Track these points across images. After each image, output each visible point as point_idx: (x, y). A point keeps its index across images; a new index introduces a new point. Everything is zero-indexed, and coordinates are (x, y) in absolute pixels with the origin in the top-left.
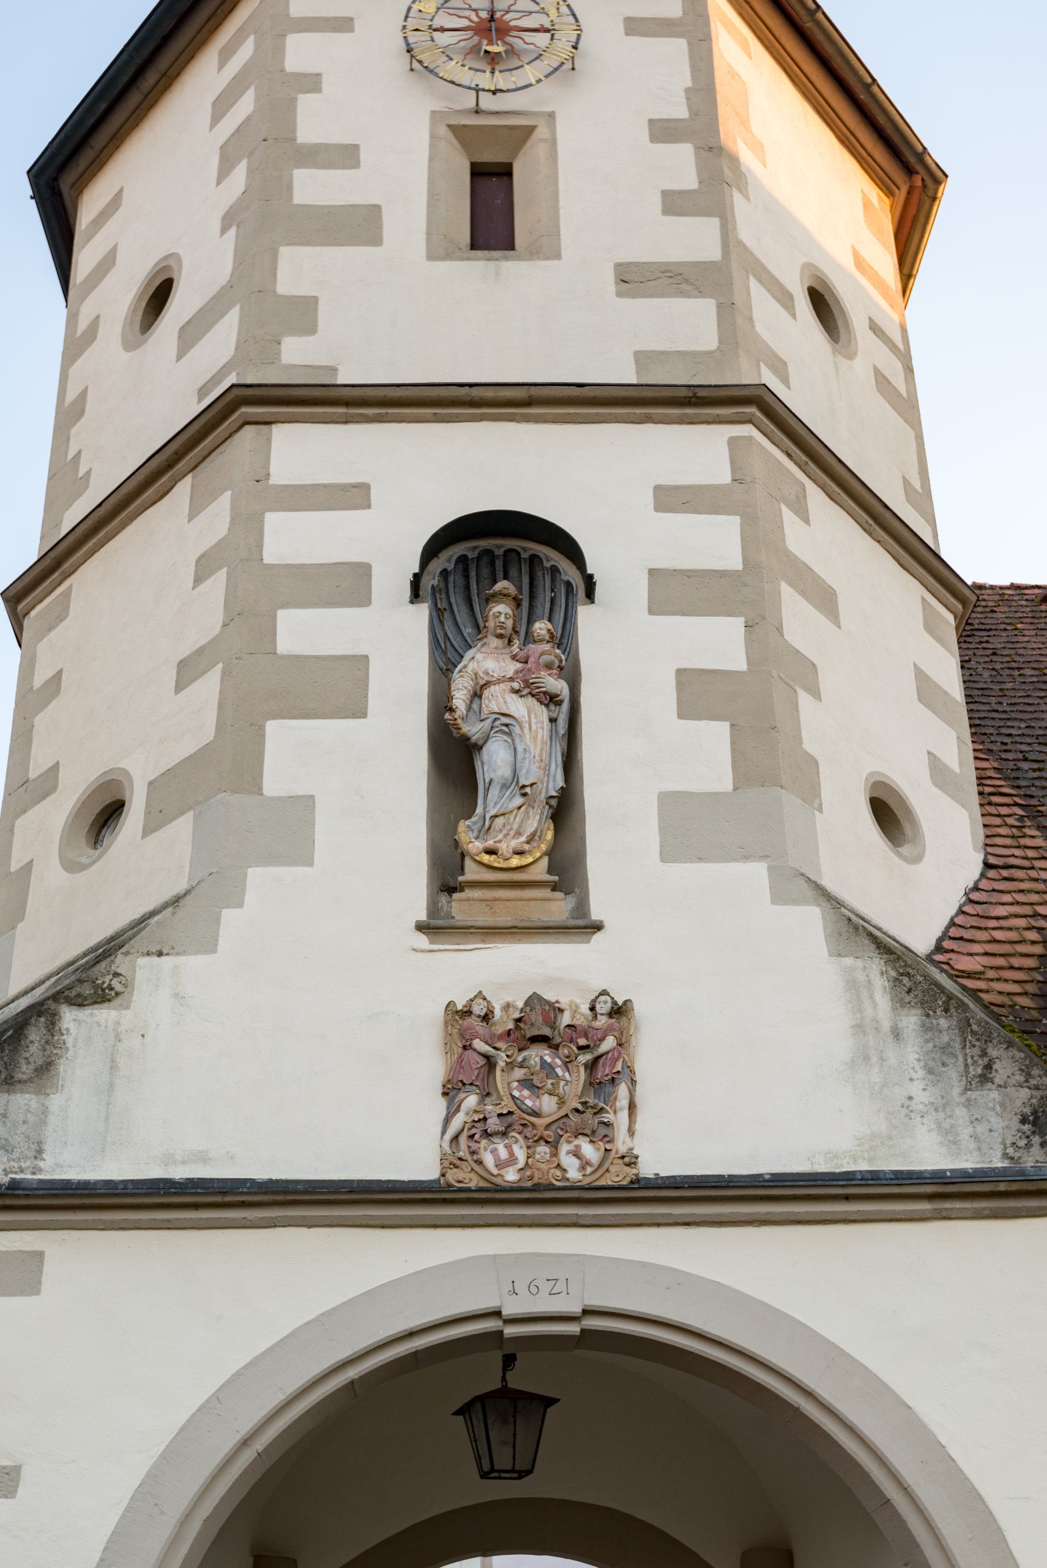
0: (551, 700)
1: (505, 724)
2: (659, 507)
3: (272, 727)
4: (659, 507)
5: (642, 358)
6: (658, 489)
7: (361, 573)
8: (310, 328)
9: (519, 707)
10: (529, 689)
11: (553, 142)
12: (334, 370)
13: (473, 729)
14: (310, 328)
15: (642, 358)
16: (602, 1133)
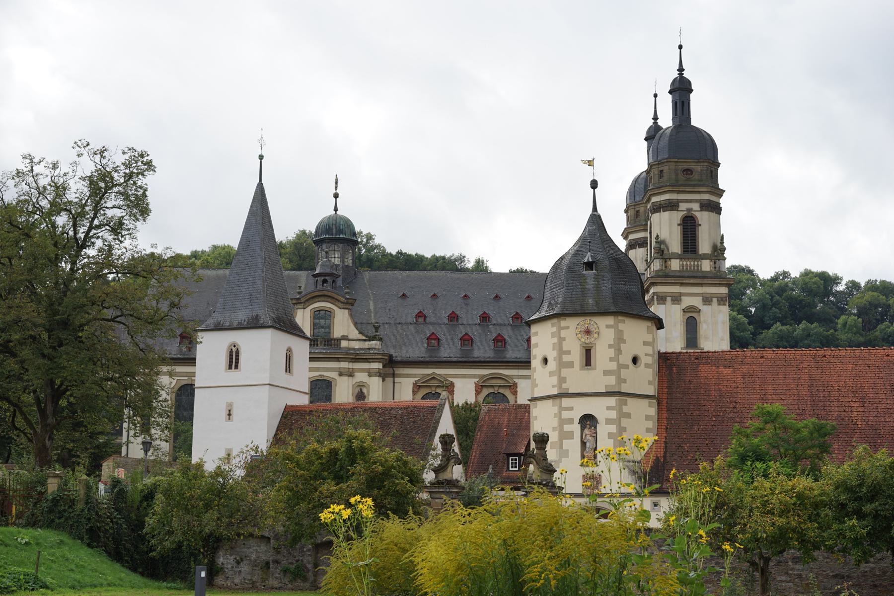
0: (594, 437)
1: (589, 441)
2: (607, 410)
3: (564, 441)
4: (607, 410)
5: (606, 386)
6: (607, 407)
7: (573, 419)
8: (565, 382)
9: (590, 438)
10: (591, 436)
11: (596, 349)
12: (568, 389)
13: (585, 441)
14: (565, 382)
15: (606, 386)
16: (598, 489)
